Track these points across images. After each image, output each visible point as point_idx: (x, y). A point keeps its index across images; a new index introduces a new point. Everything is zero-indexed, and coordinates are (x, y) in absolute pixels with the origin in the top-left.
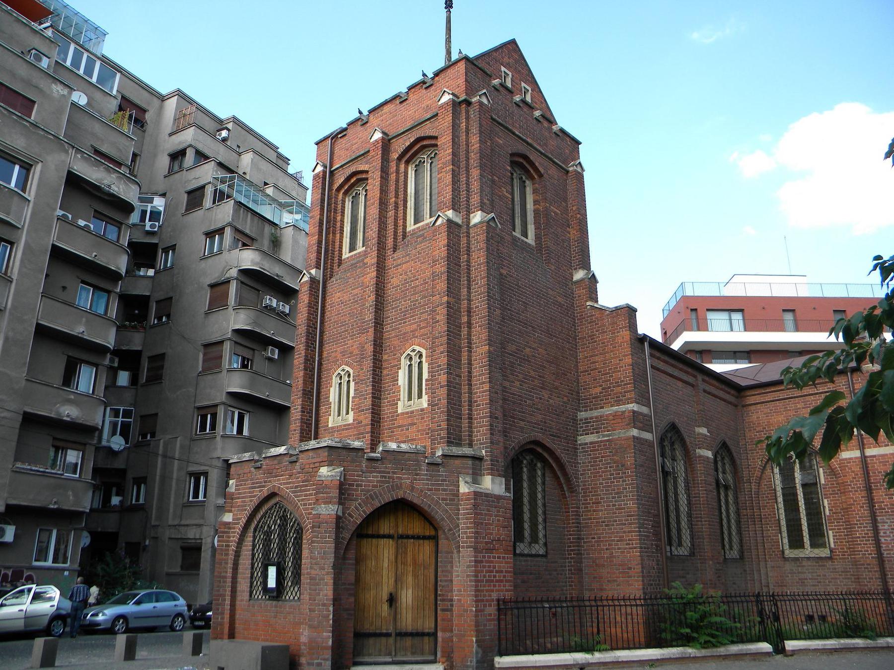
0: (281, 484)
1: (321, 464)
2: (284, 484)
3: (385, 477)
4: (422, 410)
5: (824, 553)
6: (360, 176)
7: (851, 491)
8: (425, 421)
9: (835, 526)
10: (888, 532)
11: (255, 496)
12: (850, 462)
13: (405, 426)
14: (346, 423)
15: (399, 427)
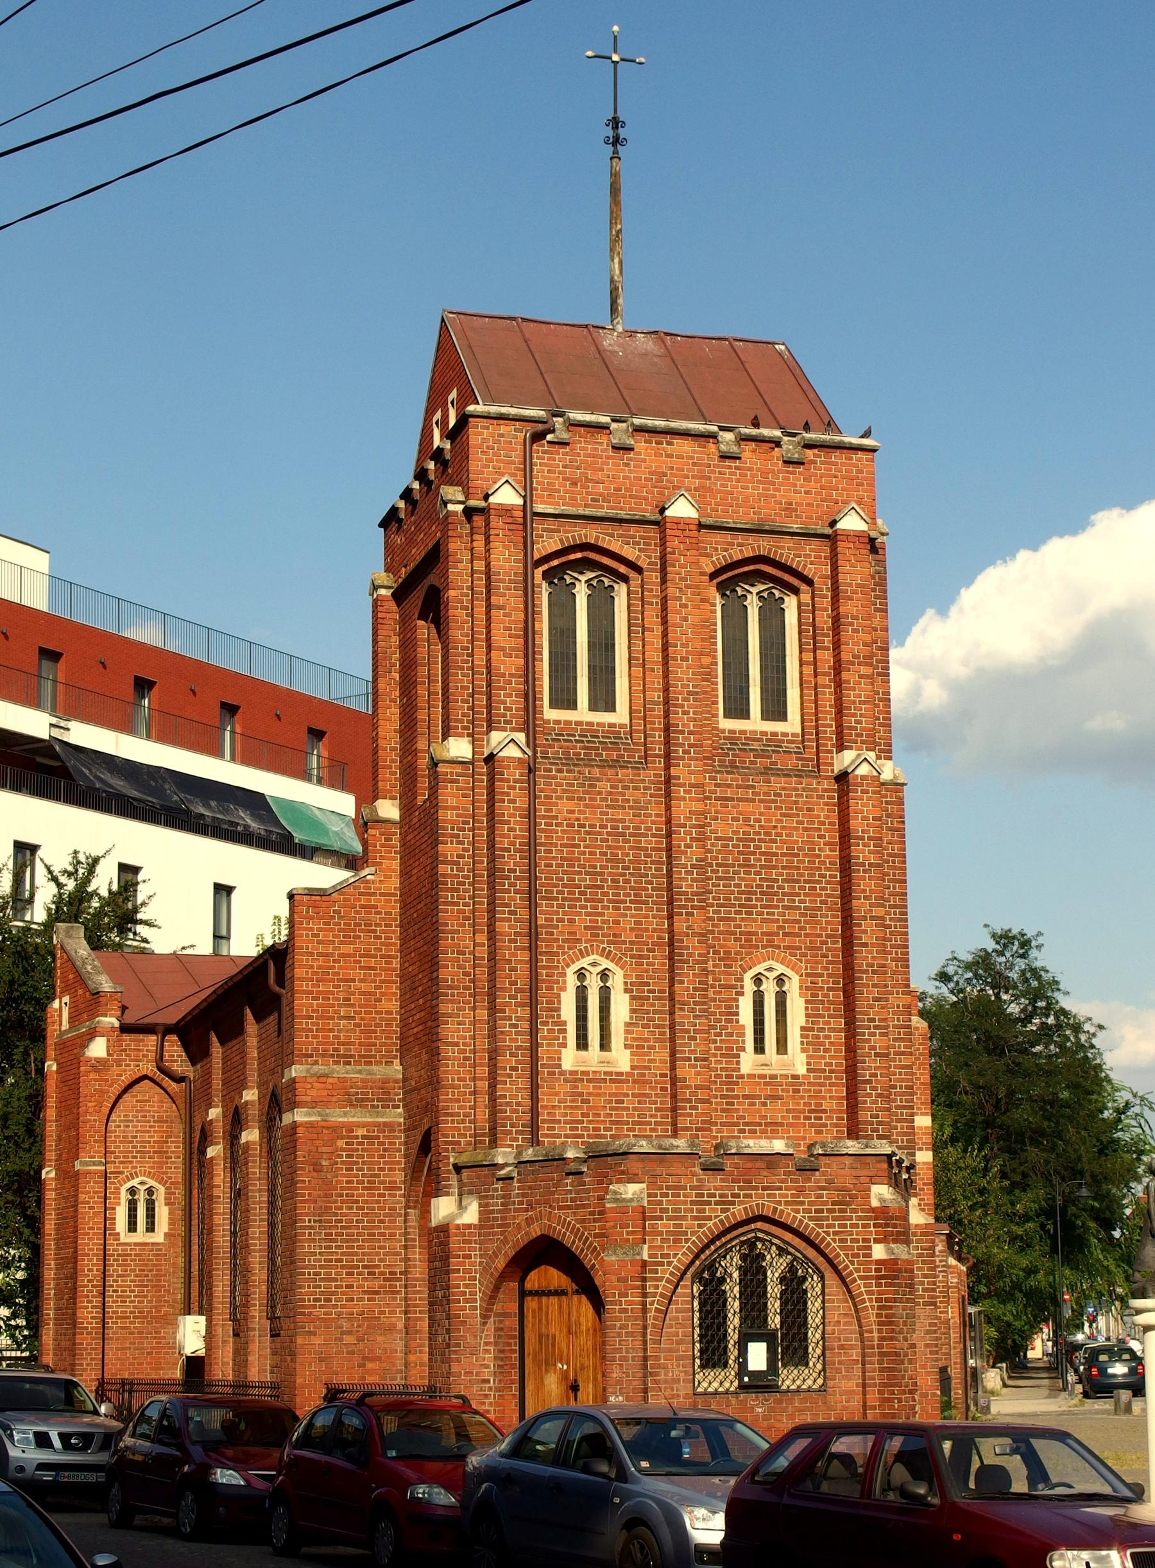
0: (779, 1203)
1: (873, 1180)
2: (787, 1203)
6: (592, 556)
8: (803, 1097)
13: (759, 1097)
15: (745, 1097)
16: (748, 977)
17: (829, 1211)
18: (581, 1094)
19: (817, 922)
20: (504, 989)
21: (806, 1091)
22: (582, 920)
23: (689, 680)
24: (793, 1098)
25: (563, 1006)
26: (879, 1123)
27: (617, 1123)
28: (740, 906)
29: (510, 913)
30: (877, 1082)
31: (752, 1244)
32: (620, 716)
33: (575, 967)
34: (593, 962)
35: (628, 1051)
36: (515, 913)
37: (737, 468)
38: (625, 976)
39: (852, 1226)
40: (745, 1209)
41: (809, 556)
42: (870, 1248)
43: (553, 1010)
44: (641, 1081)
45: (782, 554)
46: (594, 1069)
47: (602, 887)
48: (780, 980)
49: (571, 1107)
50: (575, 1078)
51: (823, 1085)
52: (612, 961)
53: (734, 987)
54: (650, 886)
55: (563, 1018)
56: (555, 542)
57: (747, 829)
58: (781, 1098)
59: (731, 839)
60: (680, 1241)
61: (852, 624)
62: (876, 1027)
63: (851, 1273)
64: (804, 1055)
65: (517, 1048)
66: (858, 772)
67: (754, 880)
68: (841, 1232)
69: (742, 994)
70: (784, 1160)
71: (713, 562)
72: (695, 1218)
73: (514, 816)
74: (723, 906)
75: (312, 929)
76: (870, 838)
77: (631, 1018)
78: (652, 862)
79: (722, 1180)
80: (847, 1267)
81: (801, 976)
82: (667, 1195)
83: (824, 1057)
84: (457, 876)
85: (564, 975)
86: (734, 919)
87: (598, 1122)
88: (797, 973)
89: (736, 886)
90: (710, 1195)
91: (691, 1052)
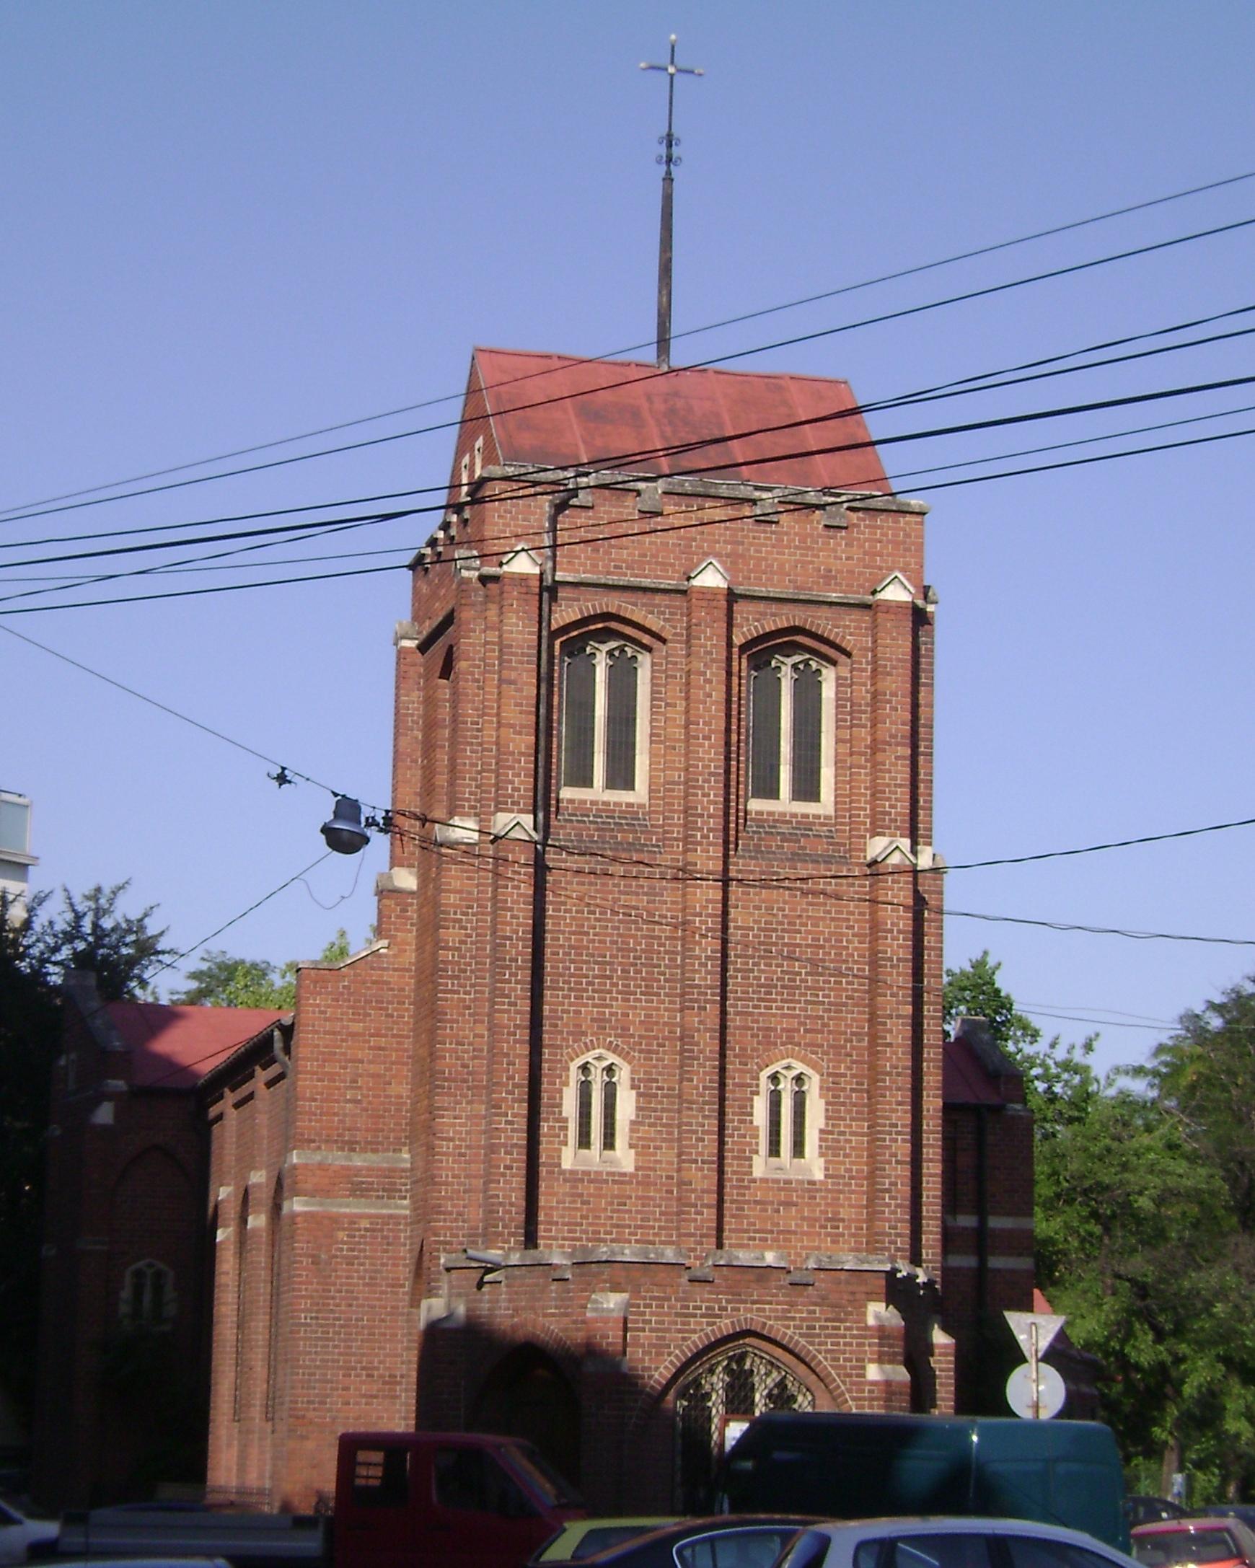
1: (871, 1296)
2: (777, 1318)
4: (812, 1183)
6: (614, 625)
8: (819, 1205)
13: (772, 1203)
14: (613, 1170)
15: (756, 1202)
18: (581, 1195)
19: (841, 1019)
21: (822, 1198)
23: (711, 760)
24: (809, 1205)
25: (564, 1102)
26: (898, 1235)
27: (618, 1226)
28: (760, 1000)
29: (510, 1004)
30: (898, 1191)
31: (741, 1359)
32: (640, 793)
33: (580, 1061)
35: (633, 1151)
37: (772, 532)
38: (632, 1072)
39: (845, 1344)
40: (733, 1323)
41: (848, 627)
42: (864, 1368)
43: (553, 1106)
44: (646, 1183)
45: (819, 625)
46: (595, 1169)
47: (610, 978)
48: (799, 1079)
49: (569, 1209)
50: (574, 1178)
51: (840, 1192)
52: (619, 1056)
53: (750, 1085)
54: (662, 978)
57: (769, 918)
58: (796, 1205)
59: (752, 929)
60: (662, 1354)
61: (890, 702)
64: (822, 1160)
67: (776, 972)
70: (776, 1273)
72: (679, 1331)
74: (740, 999)
75: (318, 1005)
77: (638, 1116)
78: (666, 952)
79: (710, 1292)
81: (822, 1075)
82: (650, 1306)
84: (458, 963)
85: (568, 1069)
86: (751, 1014)
87: (597, 1225)
88: (818, 1072)
89: (755, 978)
91: (698, 1154)
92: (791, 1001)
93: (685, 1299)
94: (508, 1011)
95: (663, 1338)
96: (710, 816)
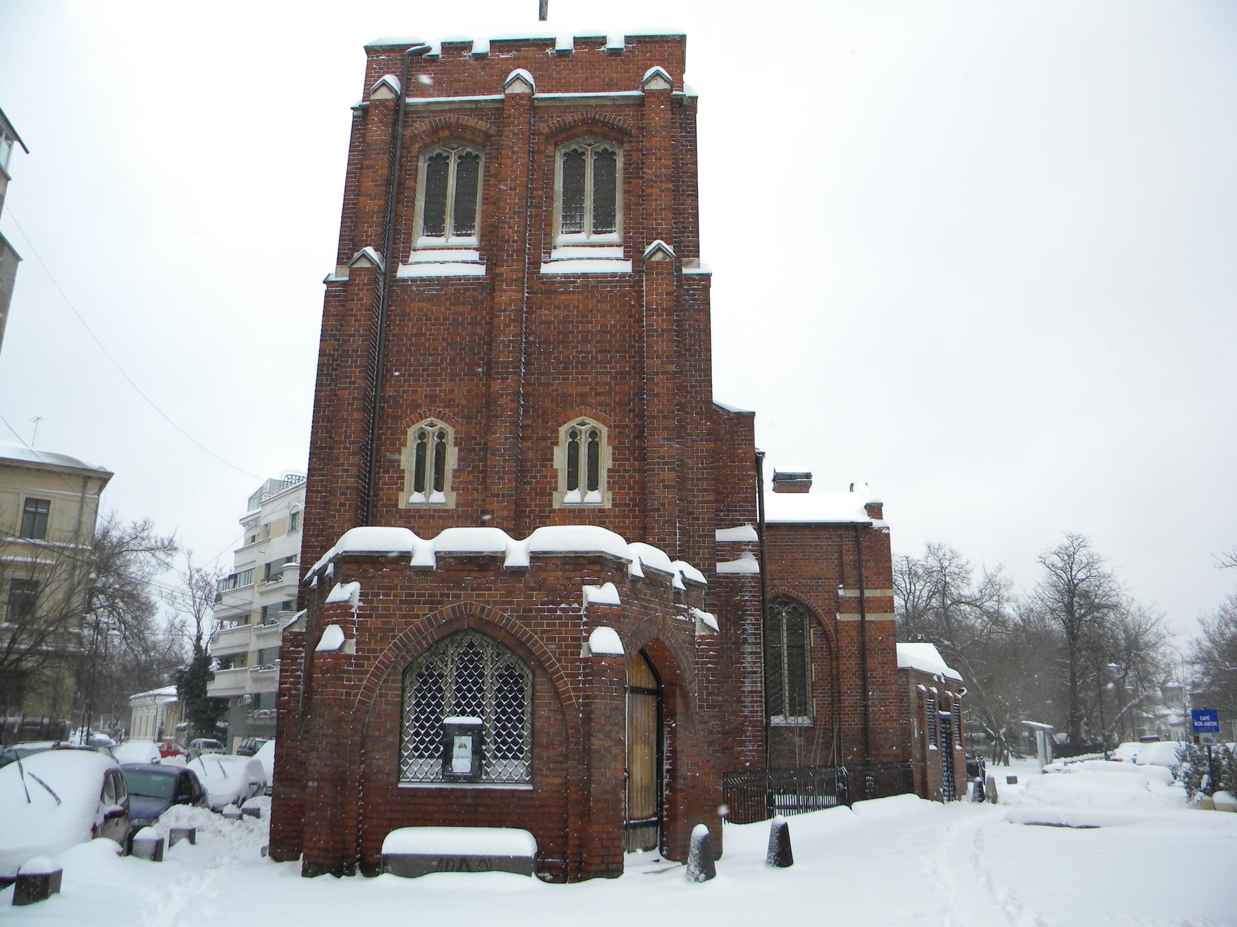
2: (495, 603)
3: (644, 607)
5: (804, 721)
7: (845, 657)
9: (820, 693)
10: (876, 702)
11: (418, 616)
12: (847, 626)
16: (563, 431)
17: (538, 610)
20: (340, 442)
22: (424, 390)
29: (351, 383)
34: (432, 425)
35: (454, 493)
36: (354, 383)
38: (455, 433)
40: (453, 609)
42: (580, 647)
52: (446, 422)
53: (549, 438)
55: (402, 468)
56: (426, 125)
62: (665, 463)
63: (558, 671)
64: (610, 493)
65: (348, 488)
66: (653, 259)
68: (549, 631)
69: (557, 444)
71: (548, 126)
72: (404, 616)
73: (360, 310)
76: (663, 309)
77: (459, 465)
79: (432, 582)
80: (553, 665)
81: (610, 427)
83: (628, 494)
84: (332, 365)
85: (406, 433)
90: (420, 595)
92: (584, 373)
93: (410, 588)
94: (348, 388)
95: (389, 622)
96: (515, 241)
